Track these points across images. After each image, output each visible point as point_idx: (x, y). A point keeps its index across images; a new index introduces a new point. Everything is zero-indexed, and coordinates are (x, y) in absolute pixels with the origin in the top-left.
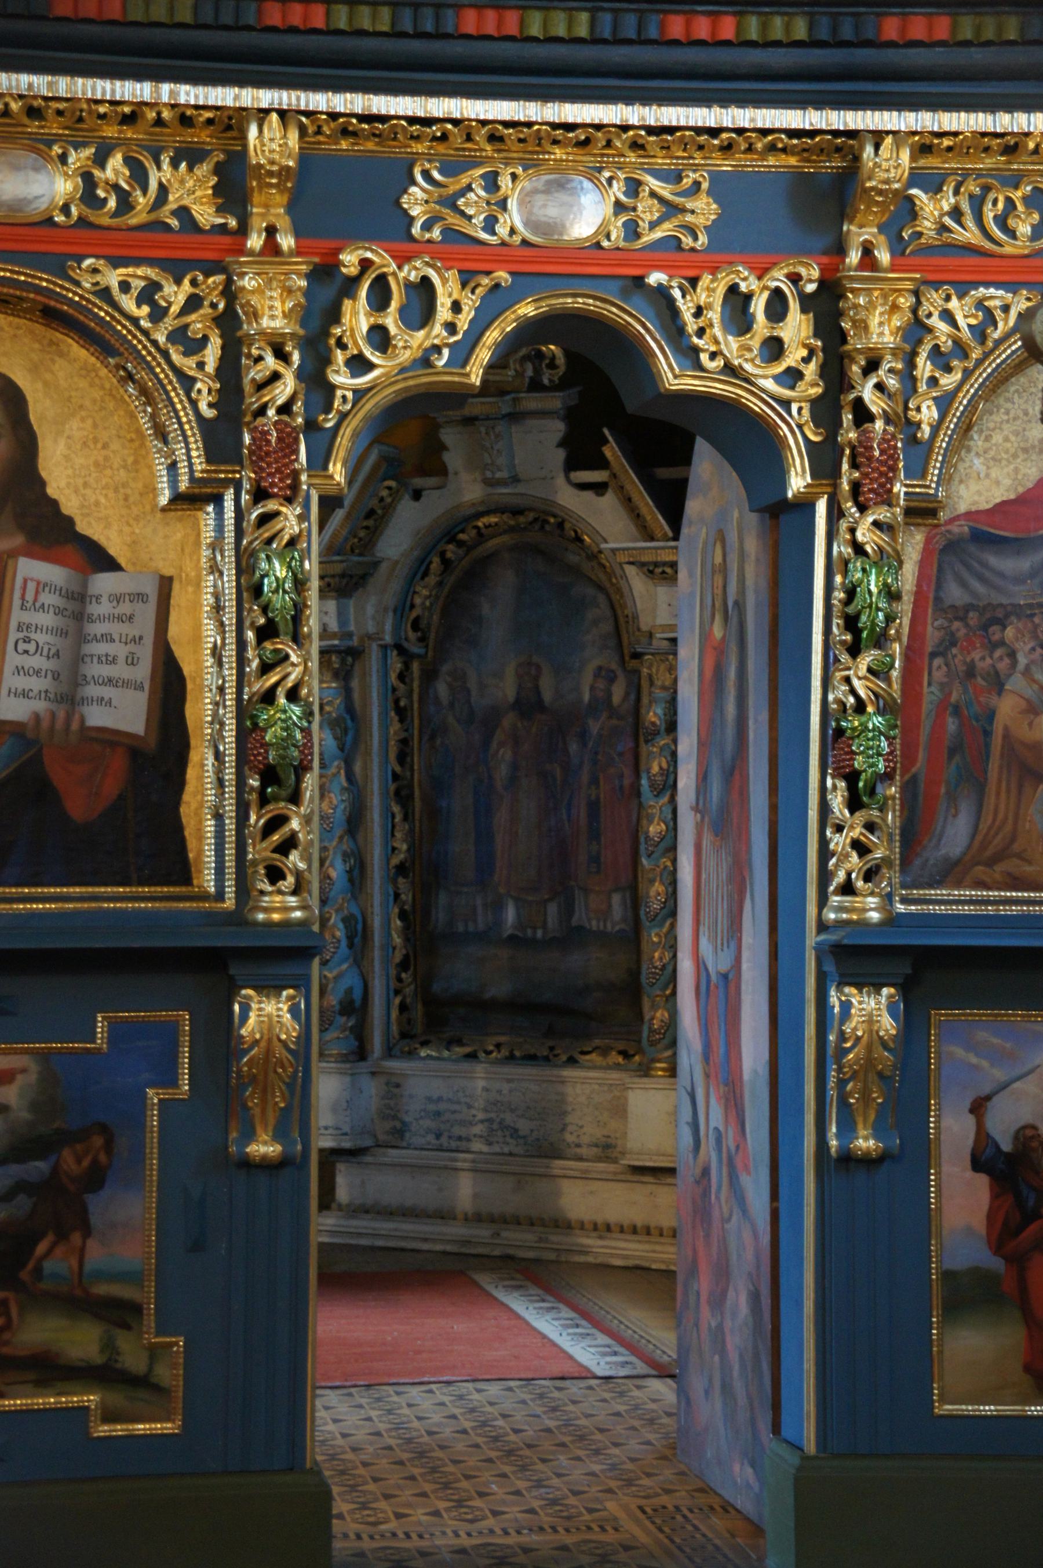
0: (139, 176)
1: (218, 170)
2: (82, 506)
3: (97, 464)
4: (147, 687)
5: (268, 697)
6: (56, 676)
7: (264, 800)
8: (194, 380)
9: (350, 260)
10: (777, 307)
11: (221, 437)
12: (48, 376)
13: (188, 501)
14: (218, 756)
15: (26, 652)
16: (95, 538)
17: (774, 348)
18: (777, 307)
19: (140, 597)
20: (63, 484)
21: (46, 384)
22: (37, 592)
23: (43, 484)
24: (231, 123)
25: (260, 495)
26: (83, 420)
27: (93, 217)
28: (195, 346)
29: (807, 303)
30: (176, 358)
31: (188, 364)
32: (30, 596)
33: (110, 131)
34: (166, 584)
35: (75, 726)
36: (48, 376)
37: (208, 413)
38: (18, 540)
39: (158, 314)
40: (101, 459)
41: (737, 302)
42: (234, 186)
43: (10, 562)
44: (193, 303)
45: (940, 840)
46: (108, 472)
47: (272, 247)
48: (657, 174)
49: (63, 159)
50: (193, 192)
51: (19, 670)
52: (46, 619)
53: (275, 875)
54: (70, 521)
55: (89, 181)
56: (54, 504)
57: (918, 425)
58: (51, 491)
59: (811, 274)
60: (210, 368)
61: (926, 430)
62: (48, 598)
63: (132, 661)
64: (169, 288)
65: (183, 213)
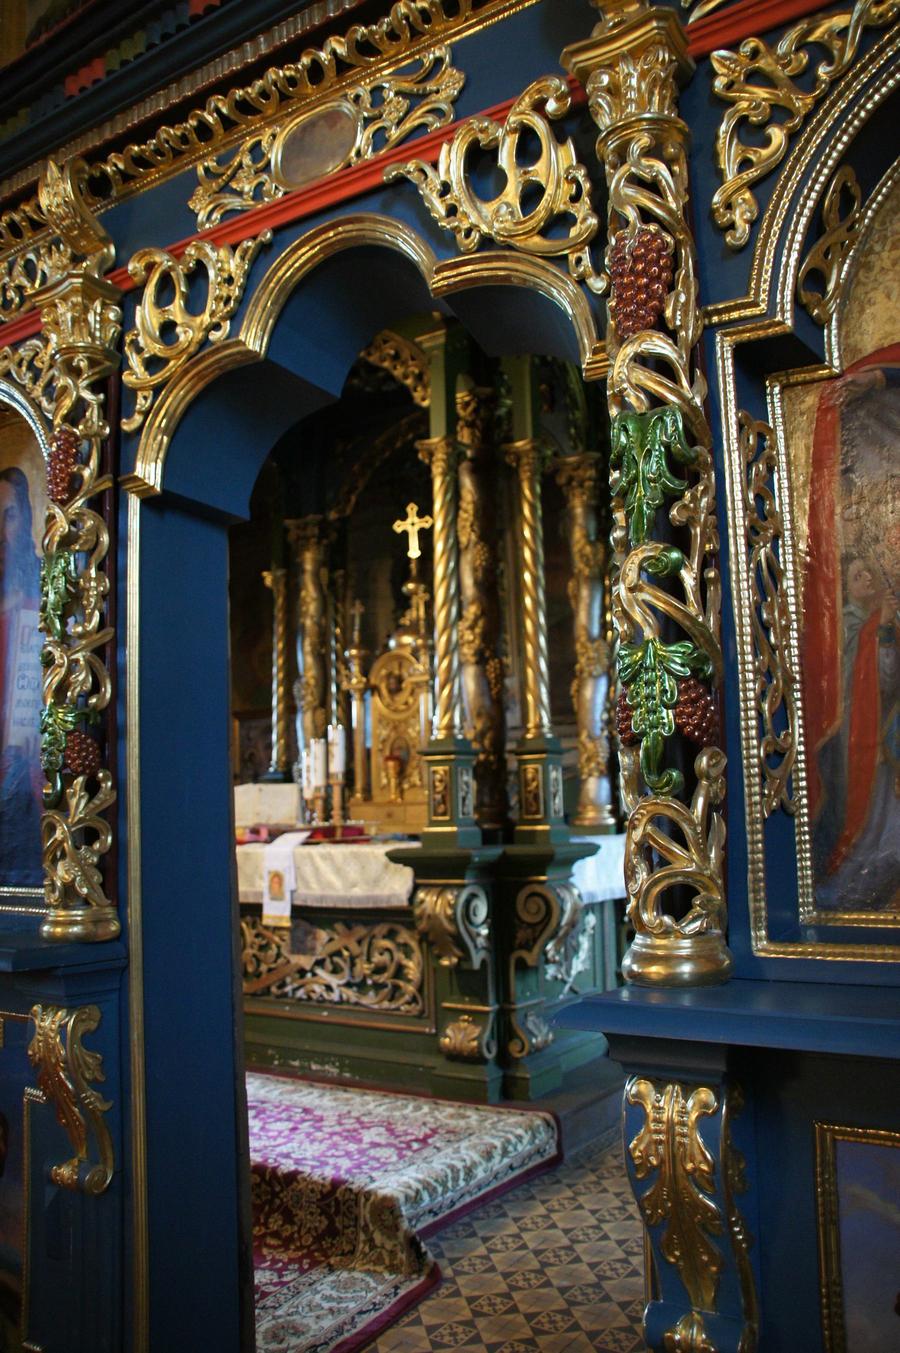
10: (528, 150)
18: (528, 150)
41: (481, 164)
45: (878, 837)
57: (732, 226)
61: (743, 229)
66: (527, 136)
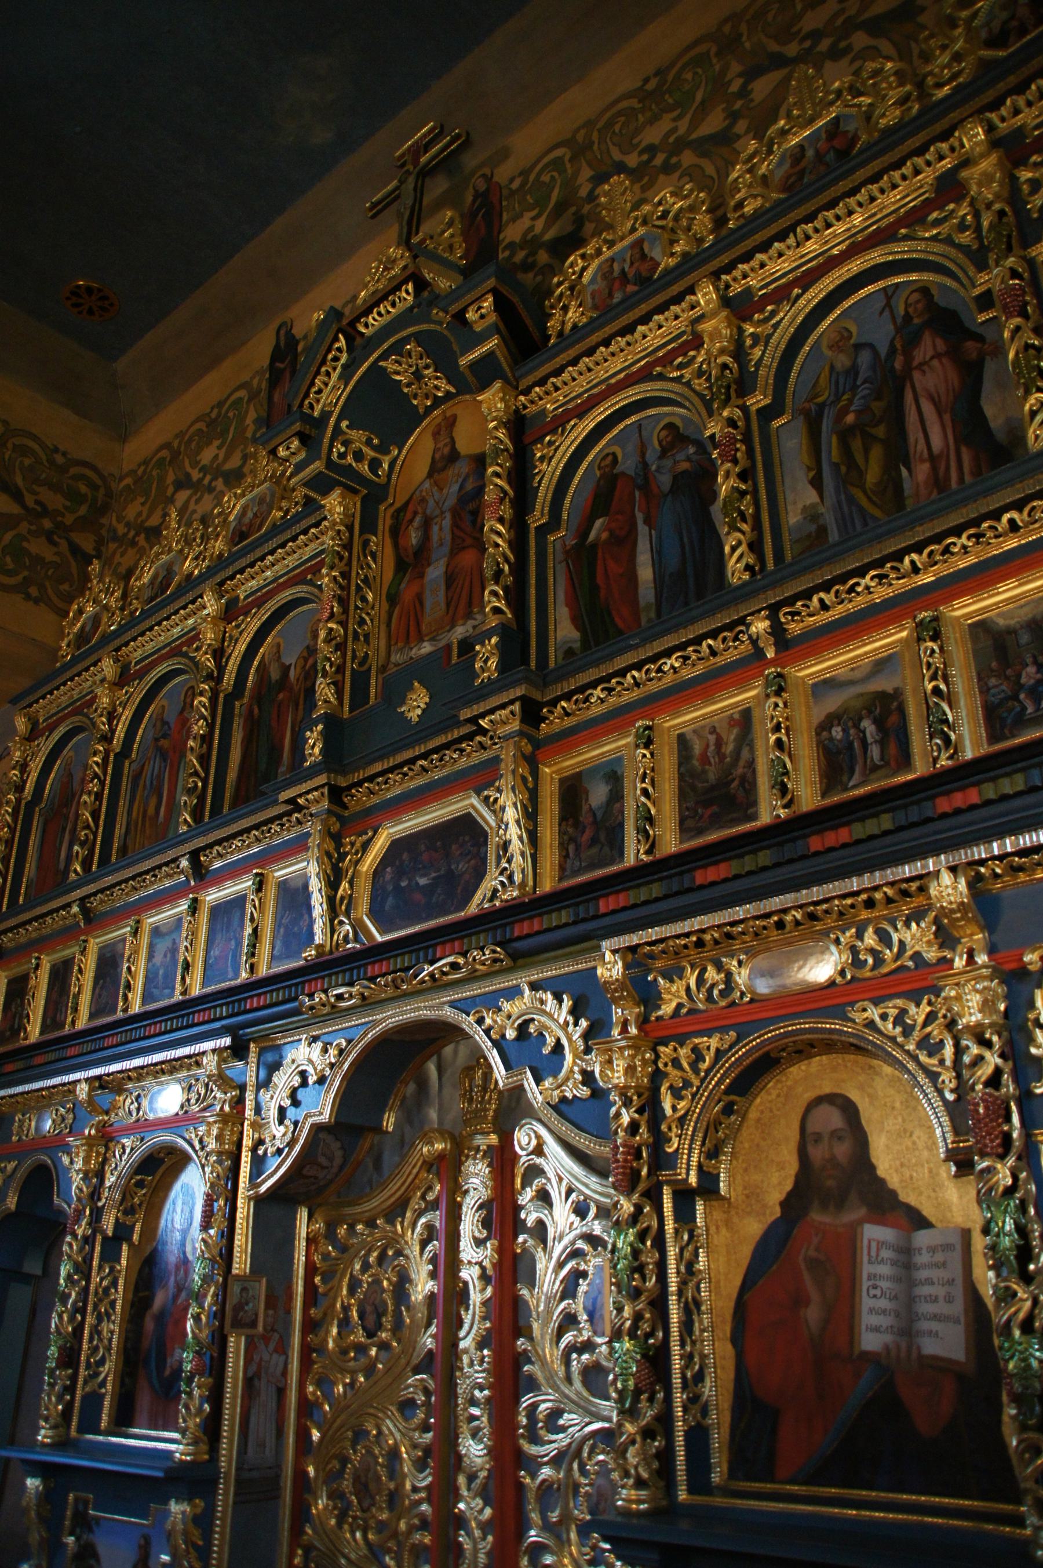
0: (884, 938)
2: (902, 1181)
3: (907, 1148)
4: (962, 1319)
6: (897, 1315)
8: (939, 1074)
12: (870, 1090)
15: (875, 1296)
16: (913, 1204)
19: (948, 1247)
20: (887, 1166)
21: (870, 1096)
22: (878, 1250)
23: (873, 1168)
26: (895, 1118)
27: (859, 974)
28: (934, 1049)
30: (923, 1058)
32: (873, 1253)
35: (914, 1355)
36: (870, 1090)
37: (950, 1097)
38: (862, 1211)
39: (907, 1031)
40: (910, 1144)
43: (859, 1230)
44: (930, 1018)
46: (917, 1153)
51: (871, 1310)
52: (885, 1270)
54: (893, 1194)
56: (882, 1182)
58: (881, 1172)
62: (886, 1254)
63: (949, 1299)
64: (912, 1010)
65: (917, 956)
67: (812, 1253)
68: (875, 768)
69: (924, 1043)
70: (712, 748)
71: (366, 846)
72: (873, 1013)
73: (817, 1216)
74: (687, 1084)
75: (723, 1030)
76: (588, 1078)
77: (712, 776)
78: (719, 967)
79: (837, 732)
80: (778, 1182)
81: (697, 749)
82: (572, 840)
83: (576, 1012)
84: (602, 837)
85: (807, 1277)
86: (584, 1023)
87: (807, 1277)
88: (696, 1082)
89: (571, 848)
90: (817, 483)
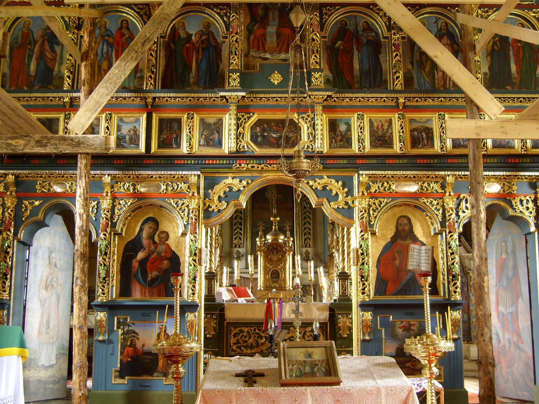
1: (441, 184)
5: (453, 264)
7: (453, 280)
9: (462, 196)
11: (443, 224)
13: (436, 234)
14: (443, 275)
17: (528, 208)
24: (444, 178)
25: (450, 232)
28: (439, 210)
29: (533, 201)
31: (437, 213)
33: (425, 179)
34: (433, 247)
37: (441, 220)
38: (411, 241)
42: (443, 187)
44: (438, 204)
47: (450, 195)
48: (507, 182)
49: (418, 183)
50: (436, 187)
53: (455, 292)
54: (418, 238)
55: (422, 186)
59: (533, 197)
60: (441, 213)
66: (528, 200)
67: (398, 249)
68: (425, 145)
69: (436, 209)
70: (380, 126)
71: (249, 118)
72: (425, 200)
73: (399, 241)
74: (377, 209)
75: (388, 198)
76: (347, 203)
77: (380, 133)
78: (388, 183)
79: (416, 133)
80: (390, 233)
81: (375, 125)
82: (333, 138)
83: (344, 186)
84: (344, 140)
85: (396, 254)
86: (346, 190)
87: (396, 254)
88: (379, 209)
89: (333, 140)
90: (412, 63)
